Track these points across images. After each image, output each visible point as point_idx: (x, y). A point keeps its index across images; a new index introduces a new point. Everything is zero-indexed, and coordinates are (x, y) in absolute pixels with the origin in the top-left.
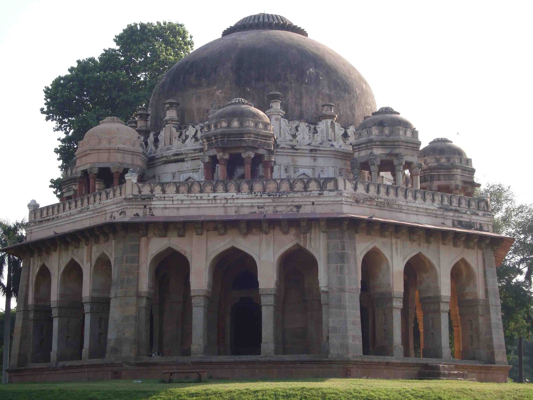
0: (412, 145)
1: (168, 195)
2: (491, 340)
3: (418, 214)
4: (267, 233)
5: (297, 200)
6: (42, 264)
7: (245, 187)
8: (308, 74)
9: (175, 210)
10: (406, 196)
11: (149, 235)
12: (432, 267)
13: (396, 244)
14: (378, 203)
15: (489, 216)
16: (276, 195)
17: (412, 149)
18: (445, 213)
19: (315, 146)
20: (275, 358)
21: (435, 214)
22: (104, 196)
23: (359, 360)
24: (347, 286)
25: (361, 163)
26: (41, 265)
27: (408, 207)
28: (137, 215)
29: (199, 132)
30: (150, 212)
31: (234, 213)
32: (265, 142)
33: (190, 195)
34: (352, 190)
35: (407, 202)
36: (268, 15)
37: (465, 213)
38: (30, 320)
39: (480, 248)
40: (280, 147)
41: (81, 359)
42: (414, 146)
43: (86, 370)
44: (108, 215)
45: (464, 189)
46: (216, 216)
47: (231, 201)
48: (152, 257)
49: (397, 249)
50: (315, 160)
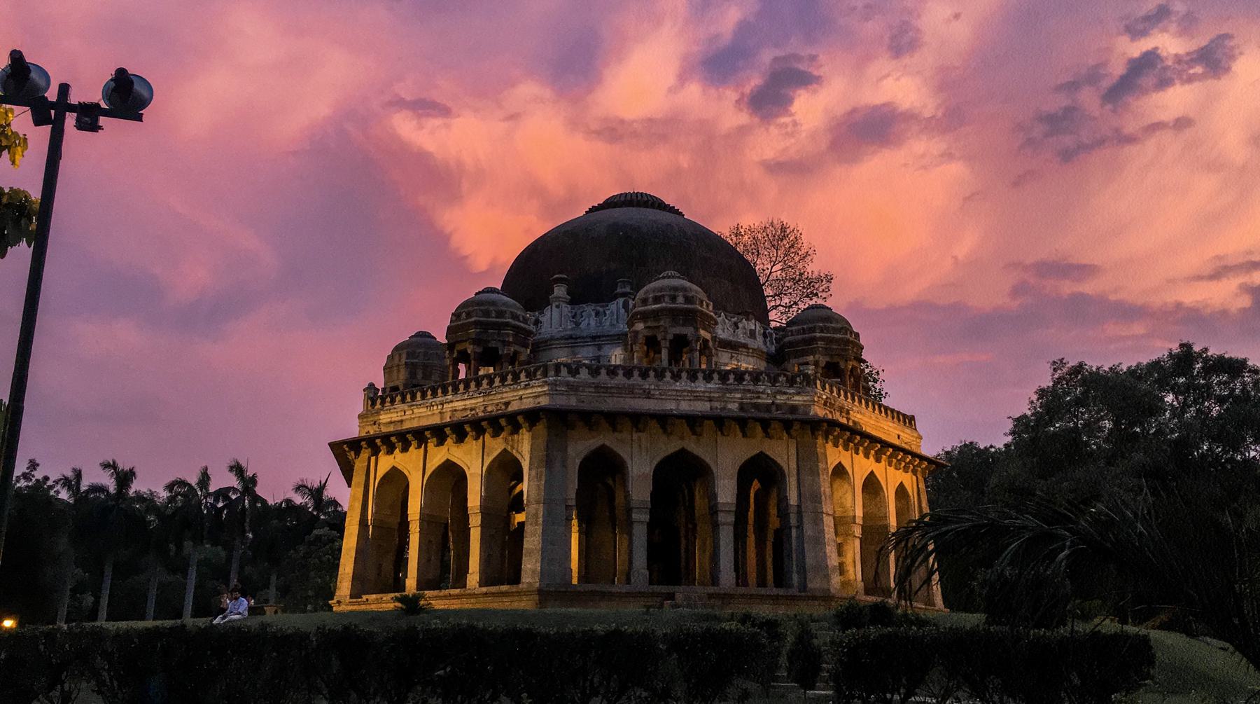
21: (709, 397)
36: (642, 193)
50: (599, 347)
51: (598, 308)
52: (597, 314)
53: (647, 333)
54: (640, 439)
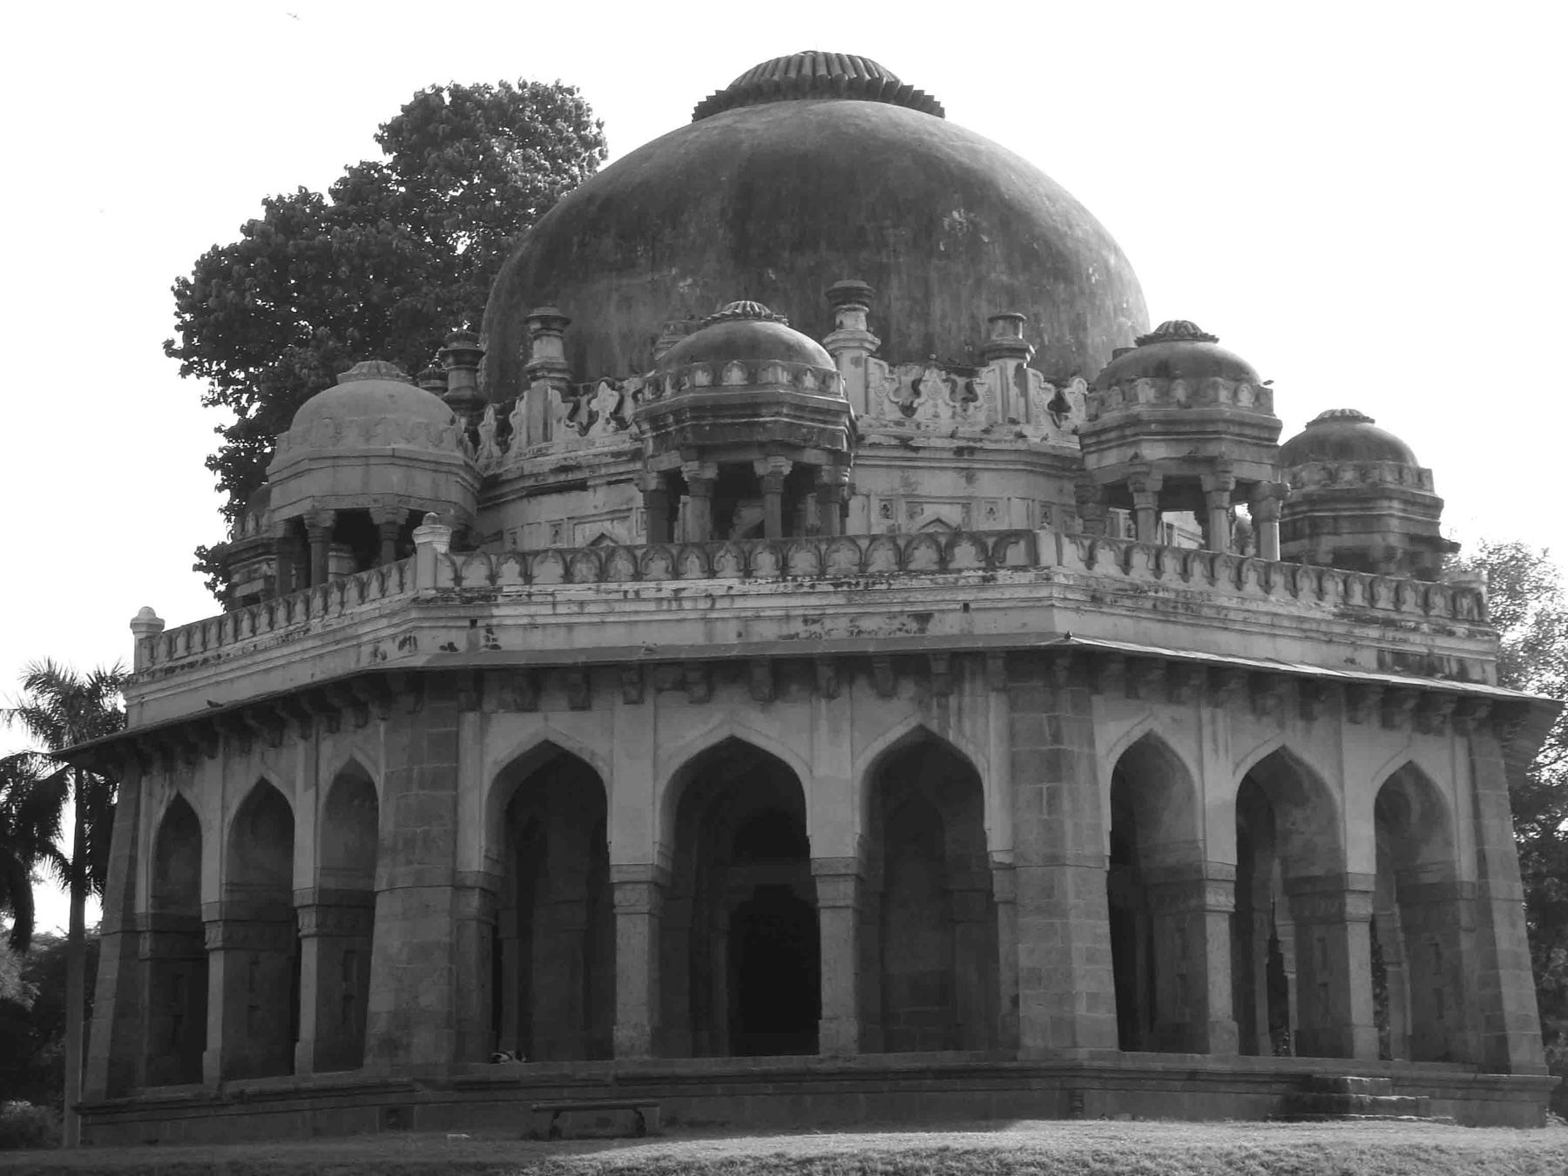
0: (1255, 432)
1: (540, 588)
2: (1498, 999)
3: (1275, 635)
4: (831, 697)
5: (920, 597)
6: (174, 793)
7: (765, 561)
8: (947, 228)
9: (562, 632)
10: (1239, 583)
11: (487, 707)
12: (1319, 787)
13: (1213, 721)
14: (1158, 604)
15: (1486, 638)
16: (858, 584)
17: (1256, 445)
18: (1357, 631)
19: (969, 439)
20: (860, 1061)
21: (1325, 634)
22: (352, 593)
23: (1107, 1064)
24: (1070, 849)
25: (1106, 487)
26: (172, 798)
27: (1246, 614)
28: (451, 647)
29: (629, 403)
30: (488, 640)
31: (732, 639)
32: (824, 429)
33: (603, 586)
34: (1081, 566)
35: (1243, 599)
36: (826, 56)
37: (1415, 630)
38: (141, 960)
39: (1461, 731)
40: (868, 441)
41: (291, 1071)
42: (1262, 435)
43: (306, 1104)
44: (367, 650)
45: (1412, 559)
46: (679, 648)
47: (724, 603)
48: (497, 770)
49: (1215, 740)
50: (970, 477)
54: (1213, 721)
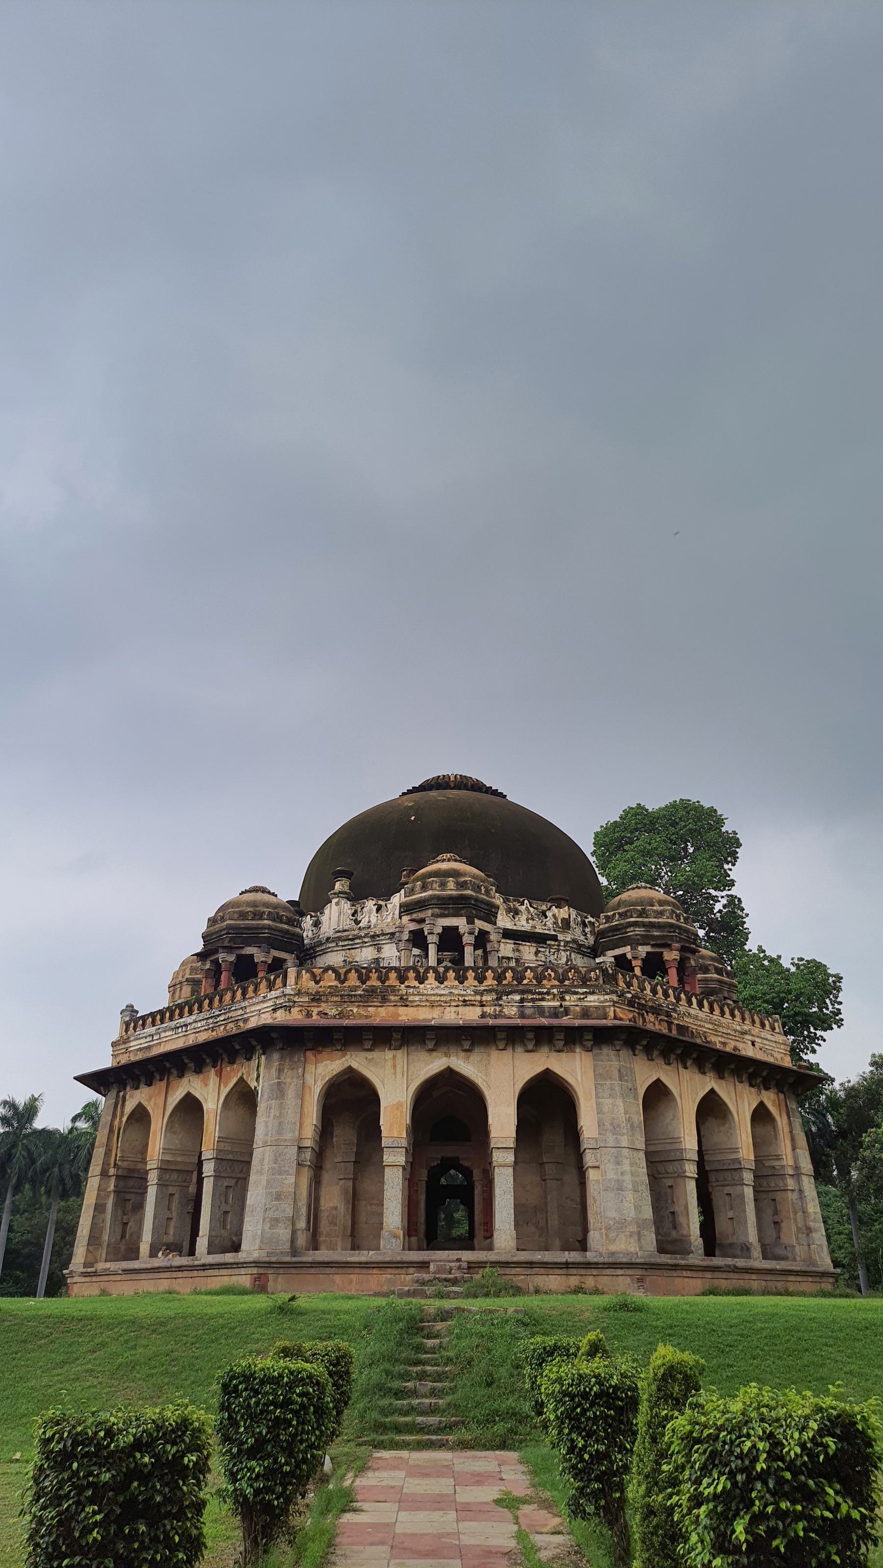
13: (394, 1057)
49: (394, 1067)
51: (380, 902)
52: (379, 909)
53: (413, 926)
